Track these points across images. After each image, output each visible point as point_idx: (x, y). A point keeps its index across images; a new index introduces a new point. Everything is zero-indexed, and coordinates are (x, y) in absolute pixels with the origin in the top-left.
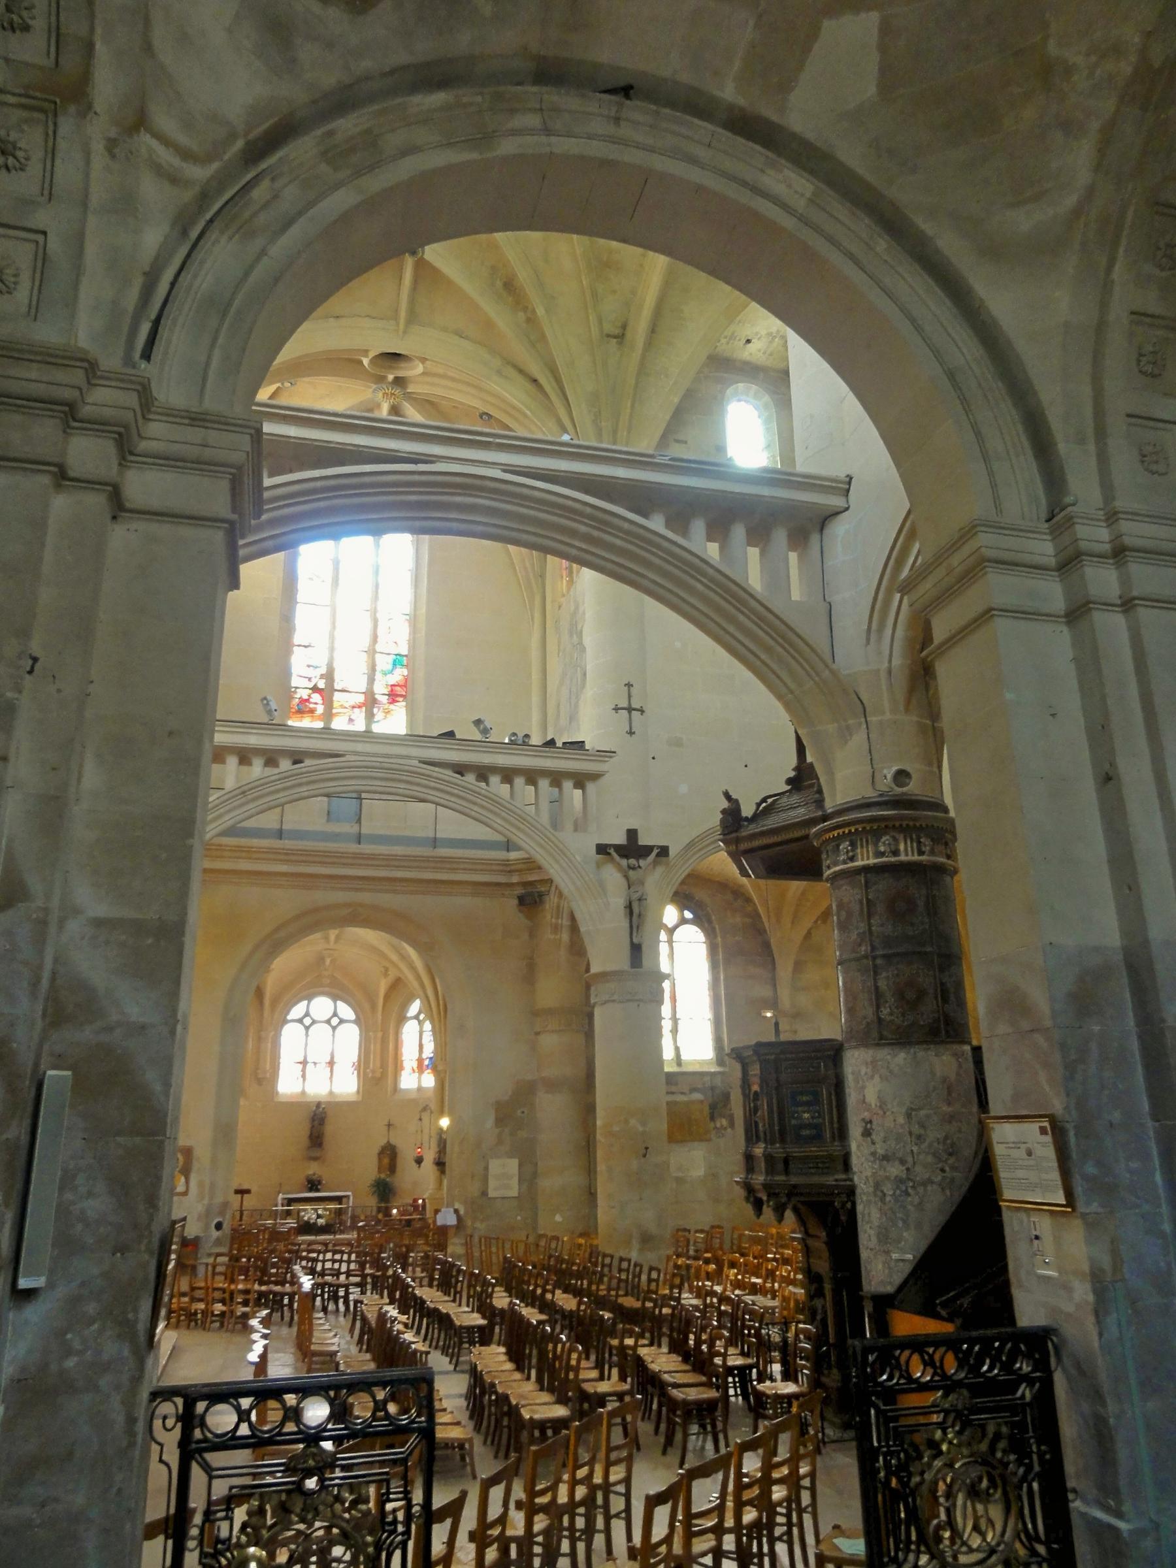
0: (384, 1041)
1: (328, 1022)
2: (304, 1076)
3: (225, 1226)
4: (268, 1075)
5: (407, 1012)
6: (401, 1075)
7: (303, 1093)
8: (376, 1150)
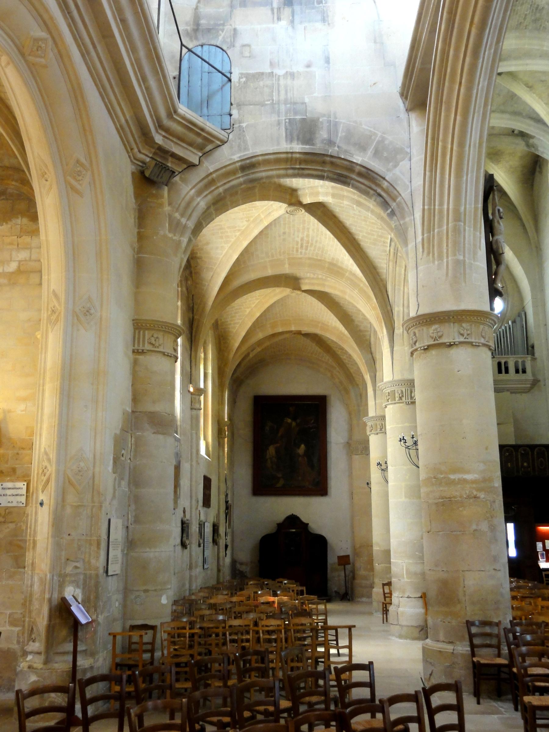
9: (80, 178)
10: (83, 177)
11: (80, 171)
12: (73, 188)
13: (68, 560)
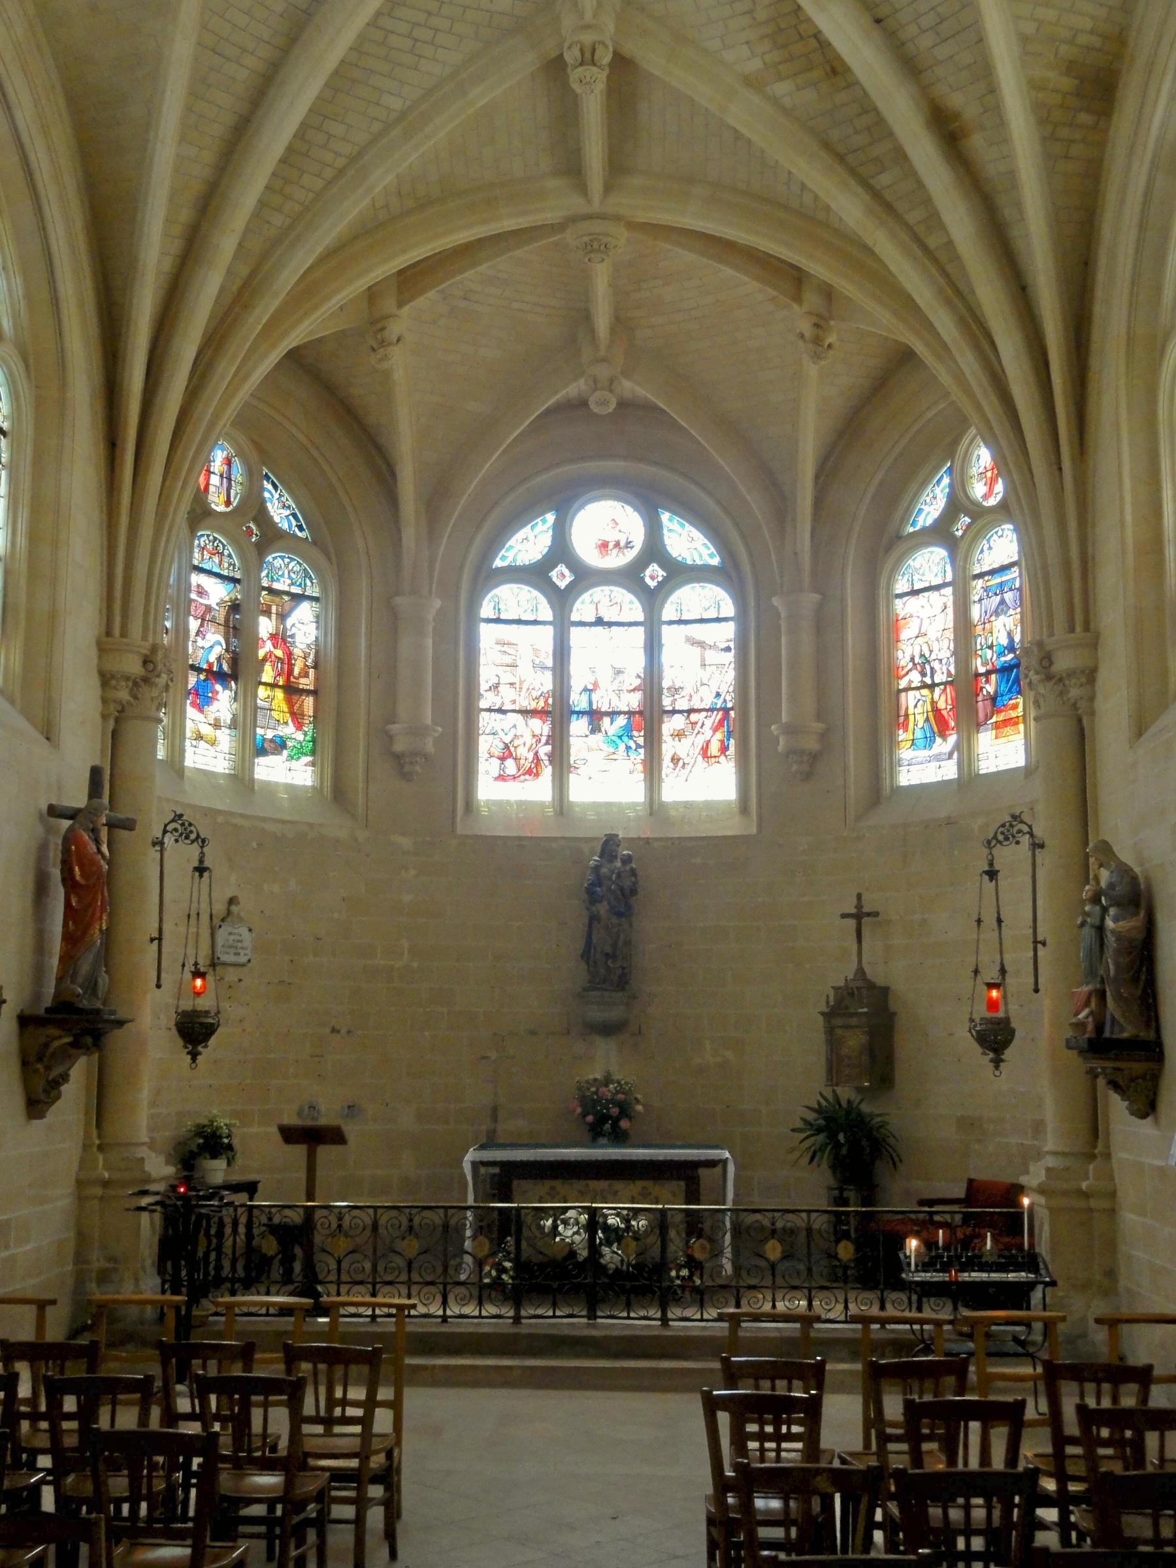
1: (630, 577)
4: (429, 746)
5: (904, 520)
6: (894, 744)
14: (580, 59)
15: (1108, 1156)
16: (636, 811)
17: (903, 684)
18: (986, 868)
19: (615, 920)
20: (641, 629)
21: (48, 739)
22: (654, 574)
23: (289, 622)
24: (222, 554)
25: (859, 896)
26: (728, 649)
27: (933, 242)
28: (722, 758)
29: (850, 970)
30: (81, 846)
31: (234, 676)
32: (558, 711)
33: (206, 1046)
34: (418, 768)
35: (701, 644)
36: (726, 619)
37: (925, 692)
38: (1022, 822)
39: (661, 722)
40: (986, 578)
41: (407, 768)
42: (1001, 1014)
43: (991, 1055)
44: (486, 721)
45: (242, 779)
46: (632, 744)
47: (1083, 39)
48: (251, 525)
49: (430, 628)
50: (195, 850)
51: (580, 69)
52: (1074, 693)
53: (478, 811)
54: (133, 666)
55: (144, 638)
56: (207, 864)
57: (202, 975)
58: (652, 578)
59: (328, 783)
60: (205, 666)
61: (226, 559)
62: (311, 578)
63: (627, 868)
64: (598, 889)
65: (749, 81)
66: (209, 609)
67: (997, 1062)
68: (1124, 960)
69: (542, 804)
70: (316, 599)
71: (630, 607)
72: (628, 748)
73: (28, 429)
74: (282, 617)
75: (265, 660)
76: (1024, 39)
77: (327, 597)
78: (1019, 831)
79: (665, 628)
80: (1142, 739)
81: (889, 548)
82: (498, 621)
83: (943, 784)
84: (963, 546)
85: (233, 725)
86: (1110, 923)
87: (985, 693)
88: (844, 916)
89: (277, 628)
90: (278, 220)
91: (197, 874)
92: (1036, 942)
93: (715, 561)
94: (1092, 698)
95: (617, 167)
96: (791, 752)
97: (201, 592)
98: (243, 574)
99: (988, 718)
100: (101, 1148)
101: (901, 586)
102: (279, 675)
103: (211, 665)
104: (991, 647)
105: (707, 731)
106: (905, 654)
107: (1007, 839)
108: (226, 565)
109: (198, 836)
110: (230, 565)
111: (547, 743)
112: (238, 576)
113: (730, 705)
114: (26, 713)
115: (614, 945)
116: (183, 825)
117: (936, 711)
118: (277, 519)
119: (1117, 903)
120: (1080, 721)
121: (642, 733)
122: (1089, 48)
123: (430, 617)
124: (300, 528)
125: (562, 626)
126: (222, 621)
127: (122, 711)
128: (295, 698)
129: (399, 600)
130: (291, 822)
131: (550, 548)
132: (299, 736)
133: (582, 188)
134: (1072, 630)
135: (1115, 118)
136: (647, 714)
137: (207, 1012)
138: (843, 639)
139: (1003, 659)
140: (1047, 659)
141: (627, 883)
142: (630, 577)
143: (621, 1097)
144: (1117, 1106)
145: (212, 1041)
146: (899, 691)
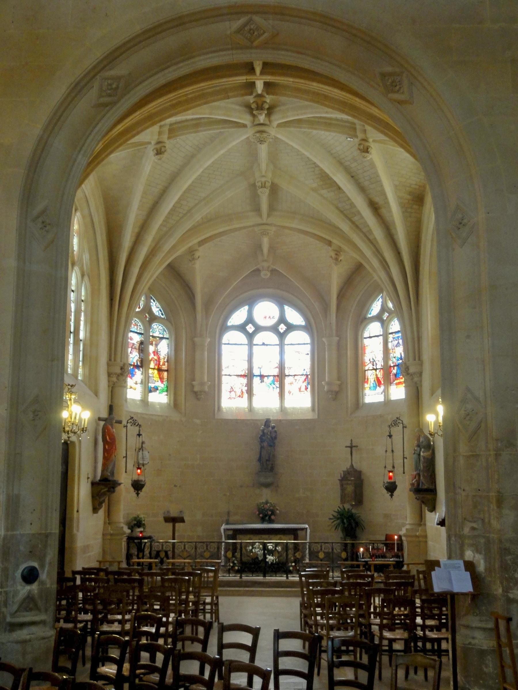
0: (340, 348)
1: (274, 329)
2: (250, 392)
3: (43, 576)
4: (206, 389)
5: (367, 311)
6: (363, 388)
7: (251, 408)
8: (338, 476)
9: (398, 88)
10: (400, 84)
11: (393, 82)
12: (400, 102)
13: (465, 519)
14: (261, 185)
15: (425, 525)
16: (276, 410)
17: (366, 368)
18: (388, 434)
19: (269, 448)
20: (278, 347)
21: (96, 396)
22: (282, 328)
23: (159, 347)
24: (137, 325)
25: (351, 440)
26: (308, 354)
27: (371, 237)
28: (306, 391)
29: (348, 465)
30: (109, 430)
31: (142, 366)
32: (249, 374)
33: (141, 491)
34: (202, 396)
35: (299, 352)
36: (307, 344)
37: (374, 371)
38: (400, 420)
39: (285, 379)
40: (394, 334)
41: (198, 397)
42: (393, 481)
43: (390, 493)
44: (224, 379)
45: (144, 401)
46: (274, 386)
47: (413, 186)
48: (147, 315)
49: (206, 349)
50: (137, 428)
51: (262, 189)
52: (416, 379)
53: (223, 411)
54: (118, 371)
55: (121, 361)
56: (141, 433)
57: (140, 469)
58: (282, 329)
59: (172, 402)
60: (132, 364)
61: (139, 327)
62: (166, 331)
63: (274, 430)
64: (264, 437)
65: (314, 190)
66: (133, 344)
67: (392, 496)
68: (425, 465)
69: (244, 408)
70: (167, 338)
71: (273, 338)
72: (273, 388)
73: (90, 299)
74: (156, 345)
75: (151, 360)
76: (396, 186)
77: (171, 337)
78: (399, 423)
79: (285, 346)
80: (434, 395)
81: (362, 322)
82: (228, 344)
83: (380, 403)
84: (386, 323)
85: (142, 383)
86: (422, 454)
87: (393, 373)
88: (346, 447)
89: (155, 349)
90: (165, 229)
91: (138, 436)
92: (404, 458)
93: (303, 323)
94: (421, 381)
95: (272, 208)
96: (329, 391)
97: (131, 339)
98: (144, 331)
99: (394, 381)
100: (109, 523)
101: (366, 335)
102: (156, 365)
103: (134, 363)
104: (395, 358)
105: (301, 383)
106: (367, 358)
107: (395, 425)
108: (139, 329)
109: (138, 424)
110: (140, 328)
111: (246, 386)
112: (142, 332)
113: (308, 373)
114: (90, 388)
115: (269, 457)
116: (133, 420)
117: (378, 378)
118: (155, 312)
119: (424, 447)
120: (417, 388)
121: (278, 383)
122: (415, 189)
123: (206, 344)
124: (162, 314)
125: (251, 345)
126: (137, 347)
127: (114, 384)
128: (161, 373)
129: (196, 339)
130: (162, 416)
131: (246, 319)
132: (162, 386)
133: (260, 216)
134: (415, 360)
135: (424, 207)
136: (280, 376)
137: (142, 481)
138: (346, 353)
139: (398, 362)
140: (407, 368)
141: (274, 435)
142: (274, 329)
143: (271, 508)
144: (426, 509)
145: (144, 489)
146: (365, 370)
